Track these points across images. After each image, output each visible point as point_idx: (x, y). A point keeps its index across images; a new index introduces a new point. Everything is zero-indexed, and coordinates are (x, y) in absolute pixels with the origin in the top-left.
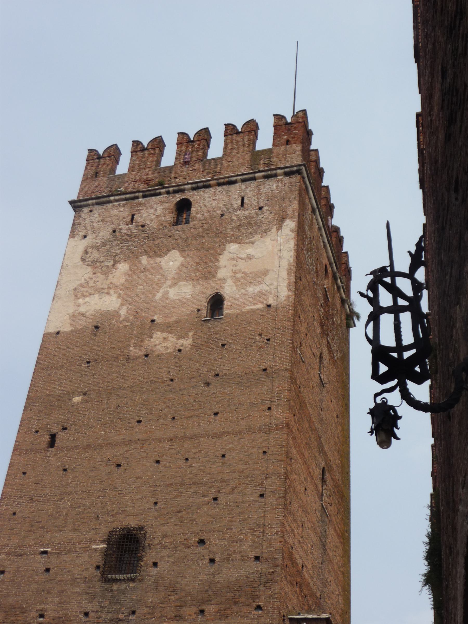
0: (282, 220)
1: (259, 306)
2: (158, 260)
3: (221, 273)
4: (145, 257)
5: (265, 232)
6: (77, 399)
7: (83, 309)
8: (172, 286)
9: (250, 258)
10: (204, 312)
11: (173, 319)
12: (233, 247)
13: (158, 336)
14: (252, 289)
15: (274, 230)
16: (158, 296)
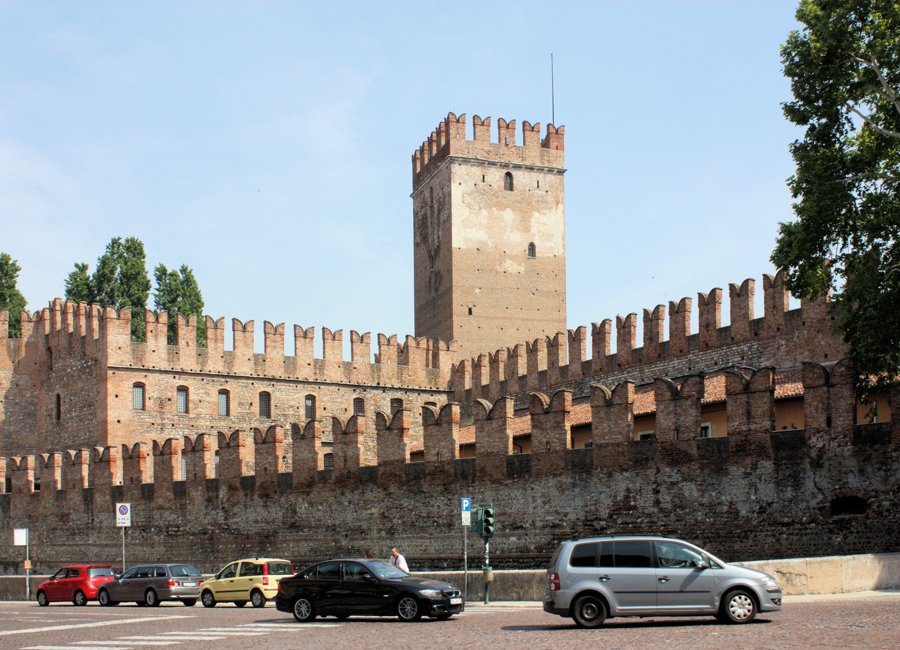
0: (558, 203)
1: (551, 255)
2: (501, 212)
3: (534, 230)
4: (494, 209)
5: (550, 209)
6: (477, 291)
7: (469, 236)
8: (511, 232)
9: (544, 224)
10: (527, 252)
11: (513, 254)
12: (536, 214)
13: (508, 261)
14: (548, 244)
15: (554, 209)
16: (505, 237)
